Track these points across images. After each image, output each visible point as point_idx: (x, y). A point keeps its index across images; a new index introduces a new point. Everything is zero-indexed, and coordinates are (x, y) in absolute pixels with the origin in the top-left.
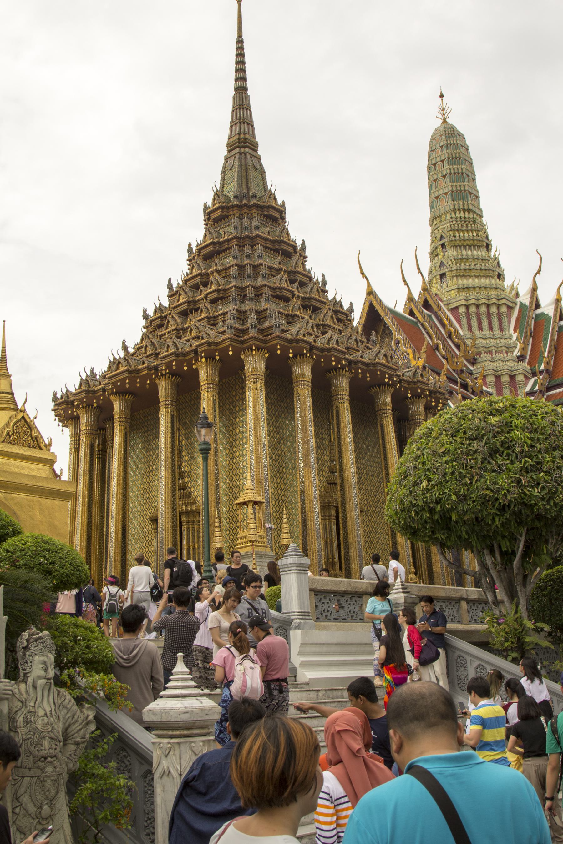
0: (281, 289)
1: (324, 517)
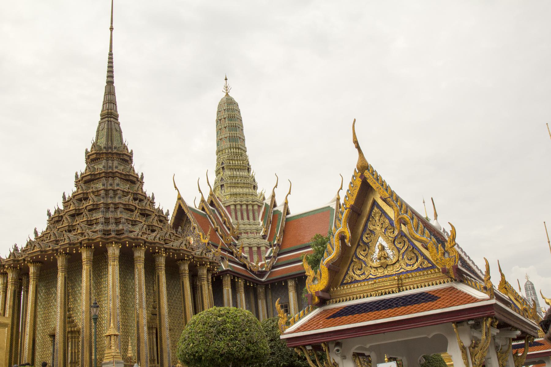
0: (129, 205)
1: (149, 334)
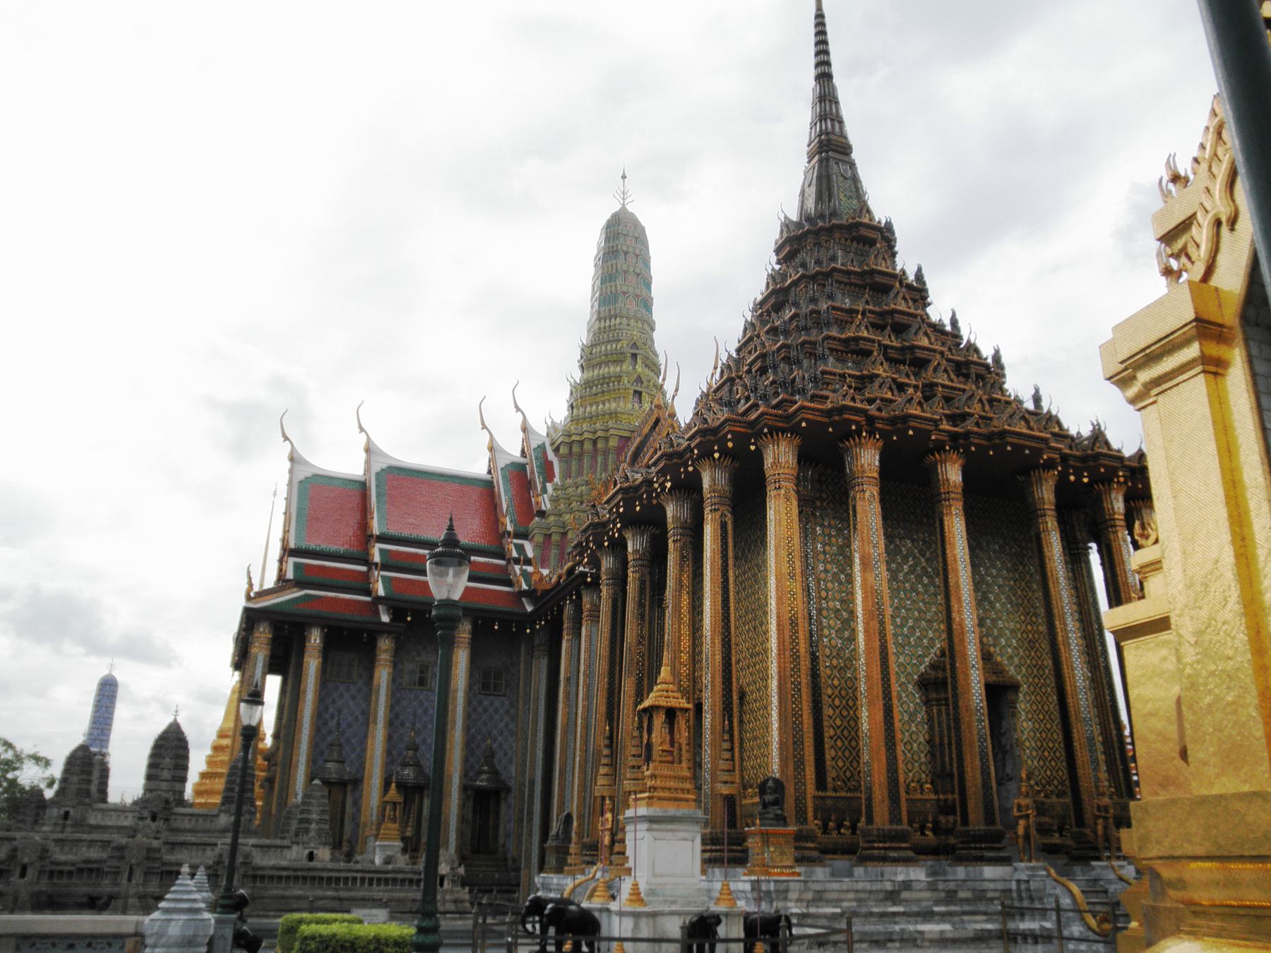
0: (856, 339)
